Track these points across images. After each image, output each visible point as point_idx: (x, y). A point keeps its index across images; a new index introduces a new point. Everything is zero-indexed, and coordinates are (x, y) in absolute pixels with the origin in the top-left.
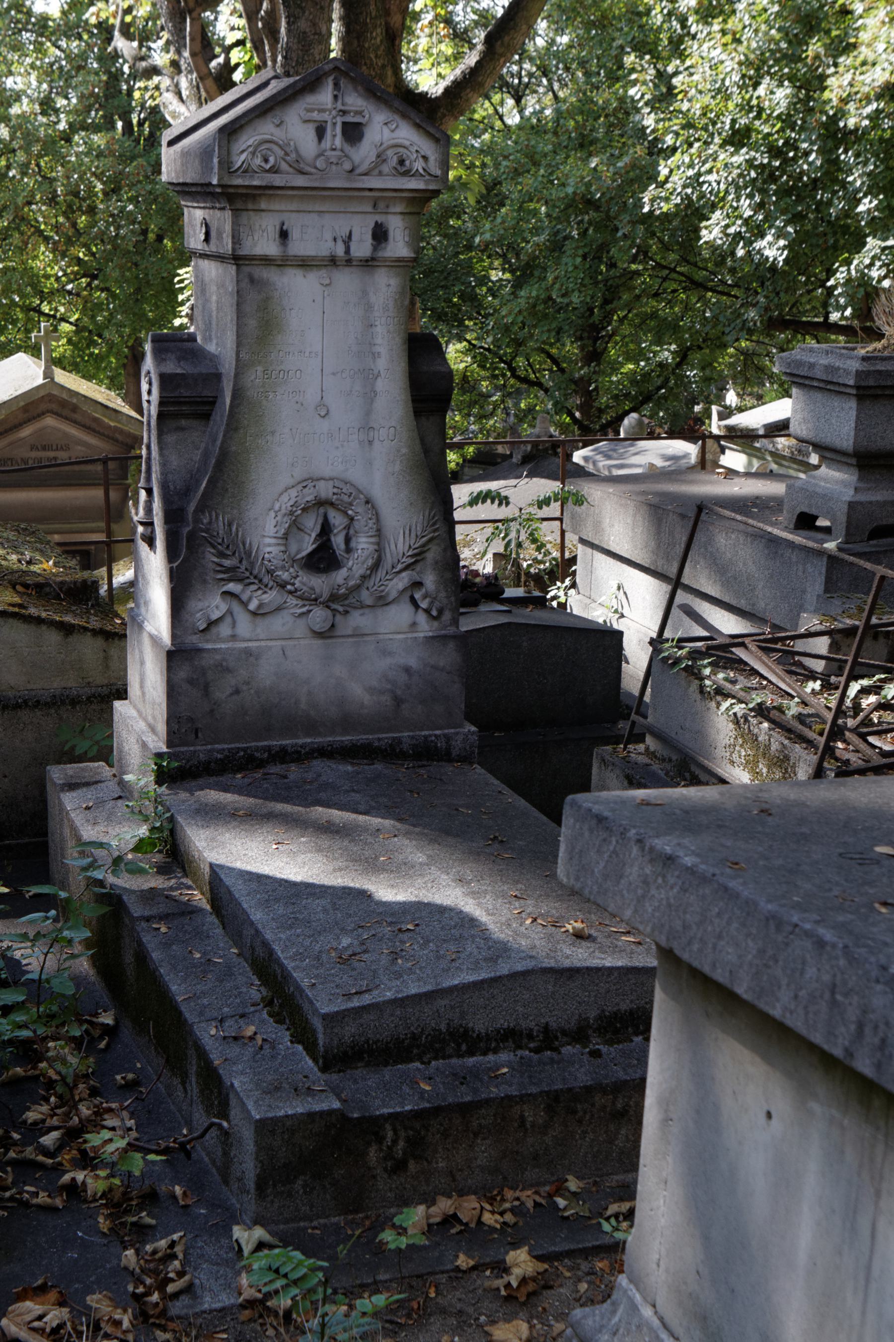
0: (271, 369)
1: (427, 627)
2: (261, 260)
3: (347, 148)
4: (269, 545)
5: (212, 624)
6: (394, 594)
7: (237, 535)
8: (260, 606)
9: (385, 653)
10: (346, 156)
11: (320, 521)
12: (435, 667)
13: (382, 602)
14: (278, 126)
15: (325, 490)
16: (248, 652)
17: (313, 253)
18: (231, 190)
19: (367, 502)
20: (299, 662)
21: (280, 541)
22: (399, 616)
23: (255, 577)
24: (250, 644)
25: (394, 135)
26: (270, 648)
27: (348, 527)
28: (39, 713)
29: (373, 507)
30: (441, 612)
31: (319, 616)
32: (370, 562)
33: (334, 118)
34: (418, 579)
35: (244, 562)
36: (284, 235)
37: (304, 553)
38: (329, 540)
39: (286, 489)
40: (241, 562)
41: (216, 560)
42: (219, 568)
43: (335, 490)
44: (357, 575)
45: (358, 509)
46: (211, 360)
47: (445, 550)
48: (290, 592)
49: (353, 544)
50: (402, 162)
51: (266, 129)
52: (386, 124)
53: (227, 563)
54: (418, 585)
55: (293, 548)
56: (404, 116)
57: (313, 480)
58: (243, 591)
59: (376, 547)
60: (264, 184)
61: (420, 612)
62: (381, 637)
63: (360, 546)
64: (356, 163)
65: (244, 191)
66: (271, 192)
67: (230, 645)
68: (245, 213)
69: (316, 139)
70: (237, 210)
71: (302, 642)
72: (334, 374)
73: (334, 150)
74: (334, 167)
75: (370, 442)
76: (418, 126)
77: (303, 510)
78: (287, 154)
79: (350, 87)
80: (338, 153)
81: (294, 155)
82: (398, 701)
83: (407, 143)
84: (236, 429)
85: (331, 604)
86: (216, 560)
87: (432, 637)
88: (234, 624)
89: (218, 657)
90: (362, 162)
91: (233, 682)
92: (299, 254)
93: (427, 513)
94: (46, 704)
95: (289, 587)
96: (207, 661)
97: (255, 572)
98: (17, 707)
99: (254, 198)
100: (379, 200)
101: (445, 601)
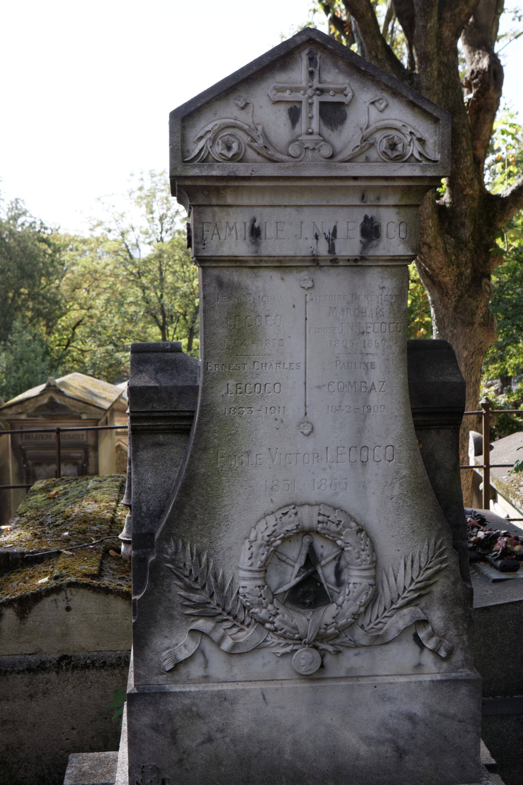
0: (244, 382)
1: (434, 669)
2: (229, 261)
3: (327, 132)
4: (244, 579)
5: (178, 665)
6: (394, 633)
7: (208, 567)
8: (235, 646)
9: (384, 698)
10: (324, 140)
11: (305, 552)
12: (444, 715)
13: (380, 641)
14: (243, 108)
15: (308, 517)
16: (222, 697)
17: (291, 253)
18: (188, 183)
19: (360, 531)
20: (282, 708)
21: (257, 575)
22: (401, 657)
23: (229, 614)
24: (226, 687)
25: (385, 115)
26: (247, 692)
27: (339, 558)
28: (104, 673)
29: (367, 535)
30: (450, 652)
31: (305, 657)
32: (363, 599)
33: (311, 97)
34: (423, 617)
35: (215, 597)
36: (255, 233)
37: (286, 587)
38: (316, 572)
39: (265, 515)
40: (211, 596)
41: (183, 593)
42: (187, 603)
43: (321, 518)
44: (348, 614)
45: (349, 539)
46: (192, 372)
47: (455, 583)
48: (269, 630)
49: (344, 577)
50: (393, 146)
51: (228, 112)
52: (373, 103)
53: (196, 597)
54: (424, 622)
55: (274, 580)
56: (395, 94)
57: (295, 505)
58: (214, 629)
59: (371, 581)
60: (225, 174)
61: (426, 652)
62: (379, 680)
63: (352, 581)
64: (338, 149)
65: (204, 183)
66: (236, 184)
67: (201, 687)
68: (209, 209)
69: (289, 123)
70: (200, 206)
71: (287, 685)
72: (319, 387)
73: (311, 134)
74: (310, 153)
75: (364, 463)
76: (412, 105)
77: (283, 539)
78: (254, 140)
79: (329, 62)
80: (316, 137)
81: (261, 141)
82: (401, 753)
83: (399, 124)
84: (205, 449)
85: (318, 644)
86: (183, 593)
87: (441, 682)
88: (206, 664)
89: (187, 701)
90: (346, 146)
91: (205, 729)
92: (274, 254)
93: (432, 542)
94: (112, 665)
95: (268, 625)
96: (174, 705)
97: (229, 608)
98: (86, 667)
99: (218, 191)
100: (368, 189)
101: (456, 640)
